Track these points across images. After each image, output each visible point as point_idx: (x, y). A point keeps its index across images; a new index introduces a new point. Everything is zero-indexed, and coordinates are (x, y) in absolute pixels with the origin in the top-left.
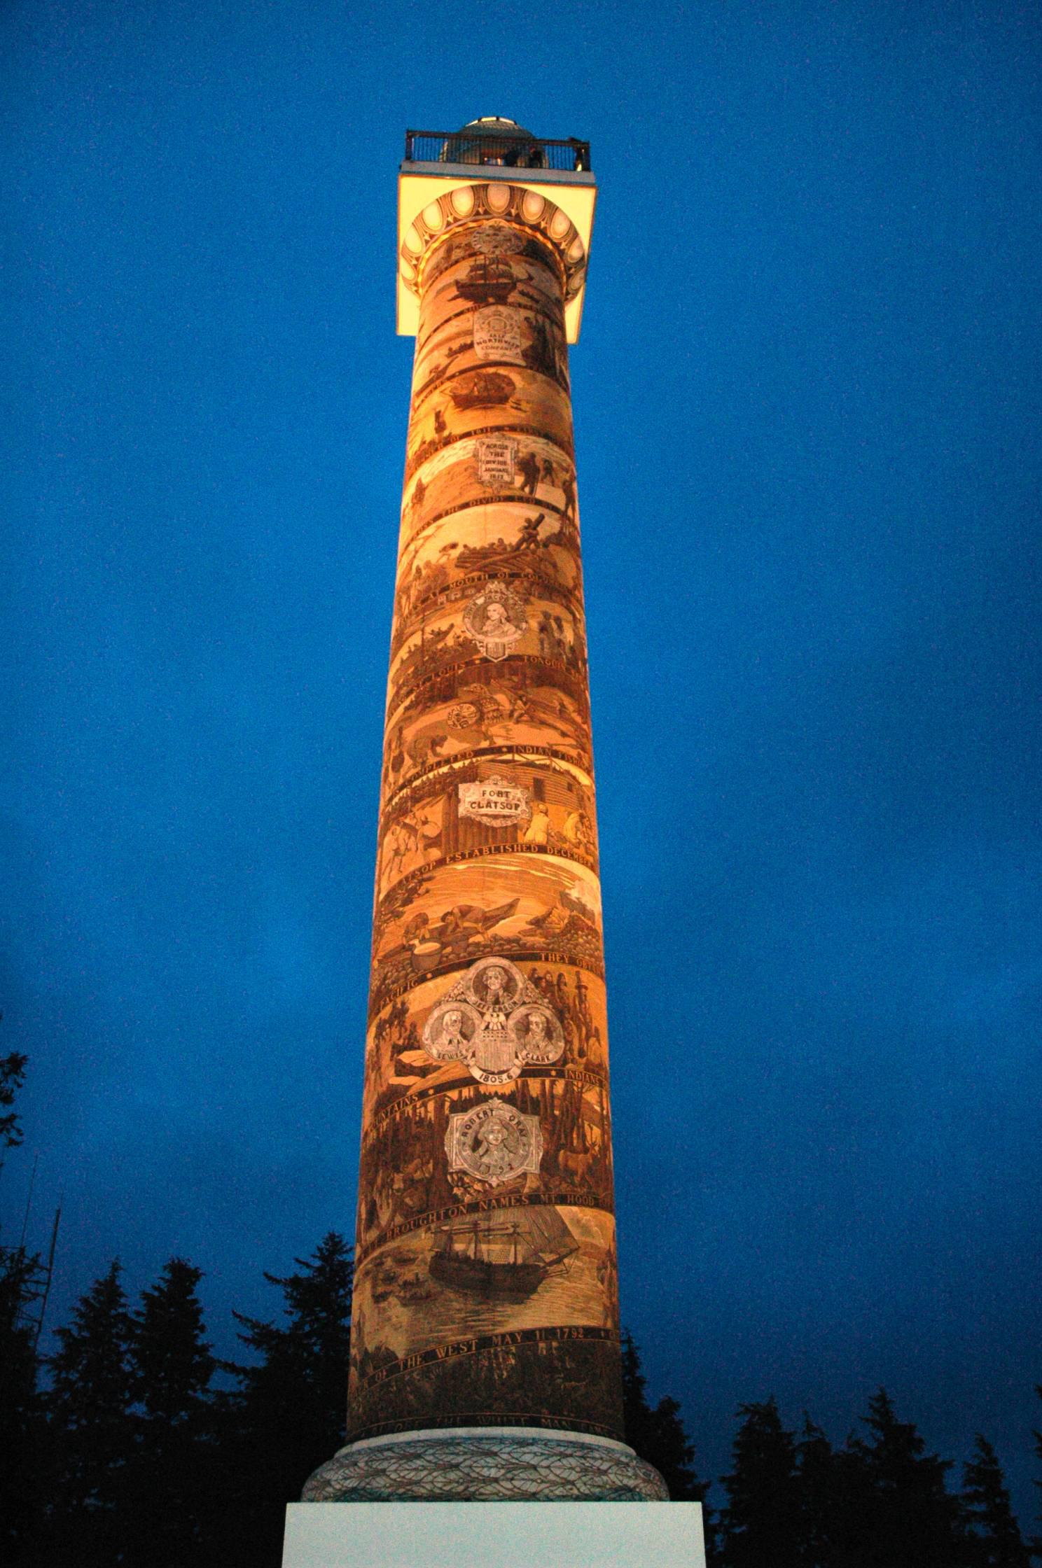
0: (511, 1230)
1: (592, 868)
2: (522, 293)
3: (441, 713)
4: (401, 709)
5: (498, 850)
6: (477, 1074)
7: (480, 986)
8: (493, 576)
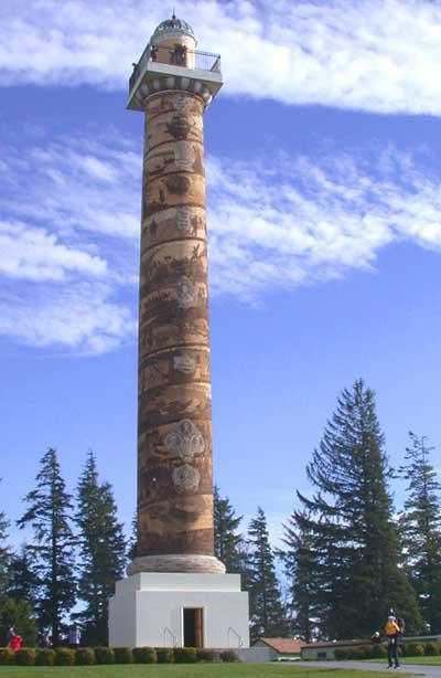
3: (166, 328)
4: (150, 321)
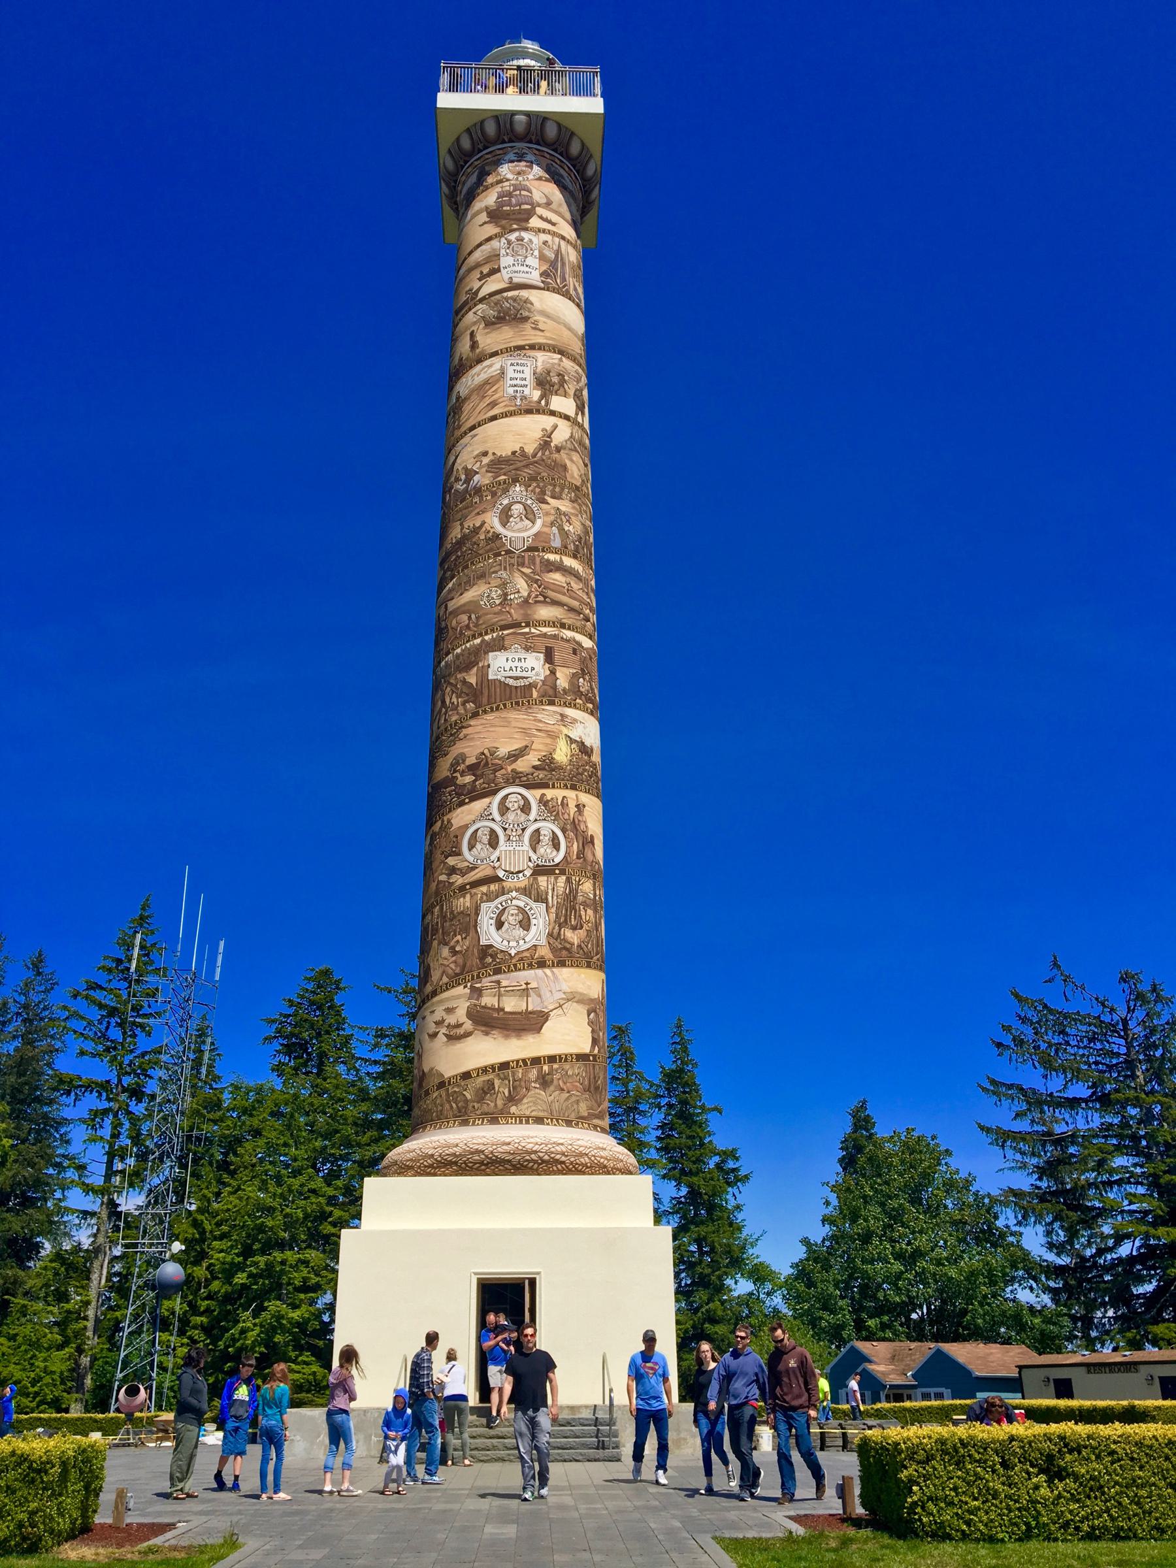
0: (524, 986)
1: (592, 714)
2: (541, 217)
5: (517, 703)
6: (501, 874)
7: (504, 809)
8: (515, 481)
